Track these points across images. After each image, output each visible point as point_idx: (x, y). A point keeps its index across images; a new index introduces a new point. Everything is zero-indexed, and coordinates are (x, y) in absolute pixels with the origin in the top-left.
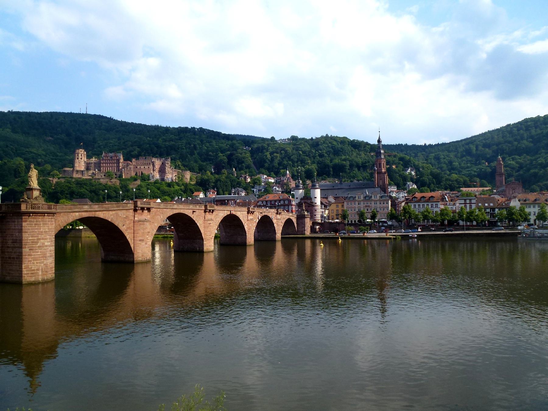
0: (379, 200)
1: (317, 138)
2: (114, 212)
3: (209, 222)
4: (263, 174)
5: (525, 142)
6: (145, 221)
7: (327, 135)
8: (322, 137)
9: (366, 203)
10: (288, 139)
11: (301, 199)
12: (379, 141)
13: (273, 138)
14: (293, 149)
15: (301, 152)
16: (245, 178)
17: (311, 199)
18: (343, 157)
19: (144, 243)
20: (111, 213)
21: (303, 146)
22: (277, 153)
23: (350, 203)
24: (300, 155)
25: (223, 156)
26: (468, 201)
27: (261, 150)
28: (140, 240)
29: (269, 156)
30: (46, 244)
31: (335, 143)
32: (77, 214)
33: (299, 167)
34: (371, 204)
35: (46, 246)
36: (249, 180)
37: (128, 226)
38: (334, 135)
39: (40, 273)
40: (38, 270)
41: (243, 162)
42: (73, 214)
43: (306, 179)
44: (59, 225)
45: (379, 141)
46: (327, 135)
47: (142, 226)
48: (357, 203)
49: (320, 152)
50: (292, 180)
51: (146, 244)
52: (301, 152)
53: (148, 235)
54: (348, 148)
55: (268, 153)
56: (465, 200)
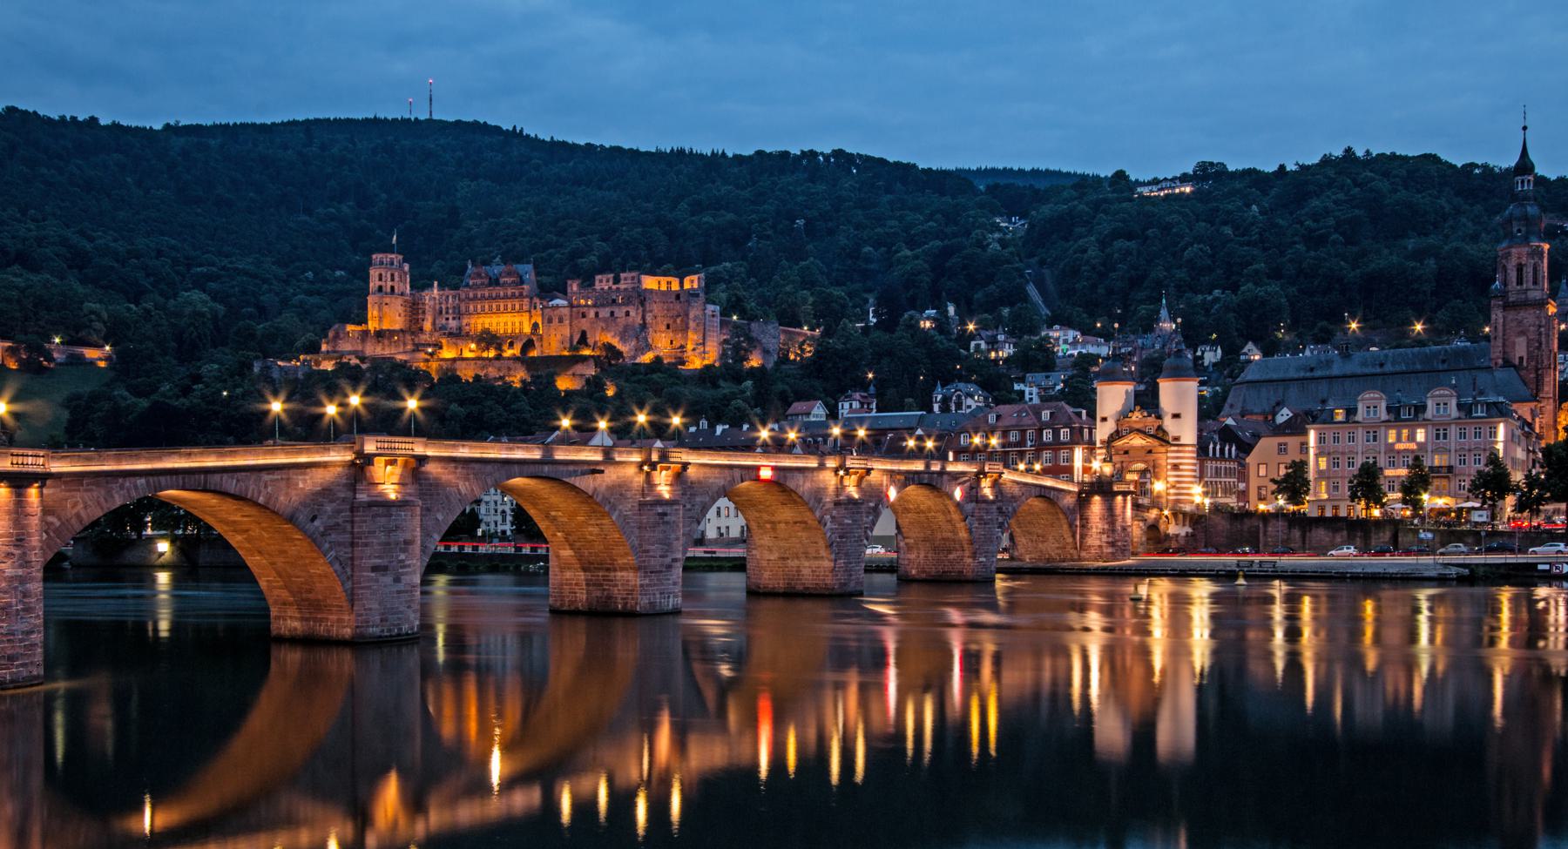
4: (1067, 323)
7: (1348, 150)
15: (1228, 230)
19: (388, 579)
25: (916, 257)
27: (1063, 227)
28: (375, 569)
29: (1093, 252)
33: (1217, 292)
46: (1348, 150)
51: (397, 580)
53: (404, 551)
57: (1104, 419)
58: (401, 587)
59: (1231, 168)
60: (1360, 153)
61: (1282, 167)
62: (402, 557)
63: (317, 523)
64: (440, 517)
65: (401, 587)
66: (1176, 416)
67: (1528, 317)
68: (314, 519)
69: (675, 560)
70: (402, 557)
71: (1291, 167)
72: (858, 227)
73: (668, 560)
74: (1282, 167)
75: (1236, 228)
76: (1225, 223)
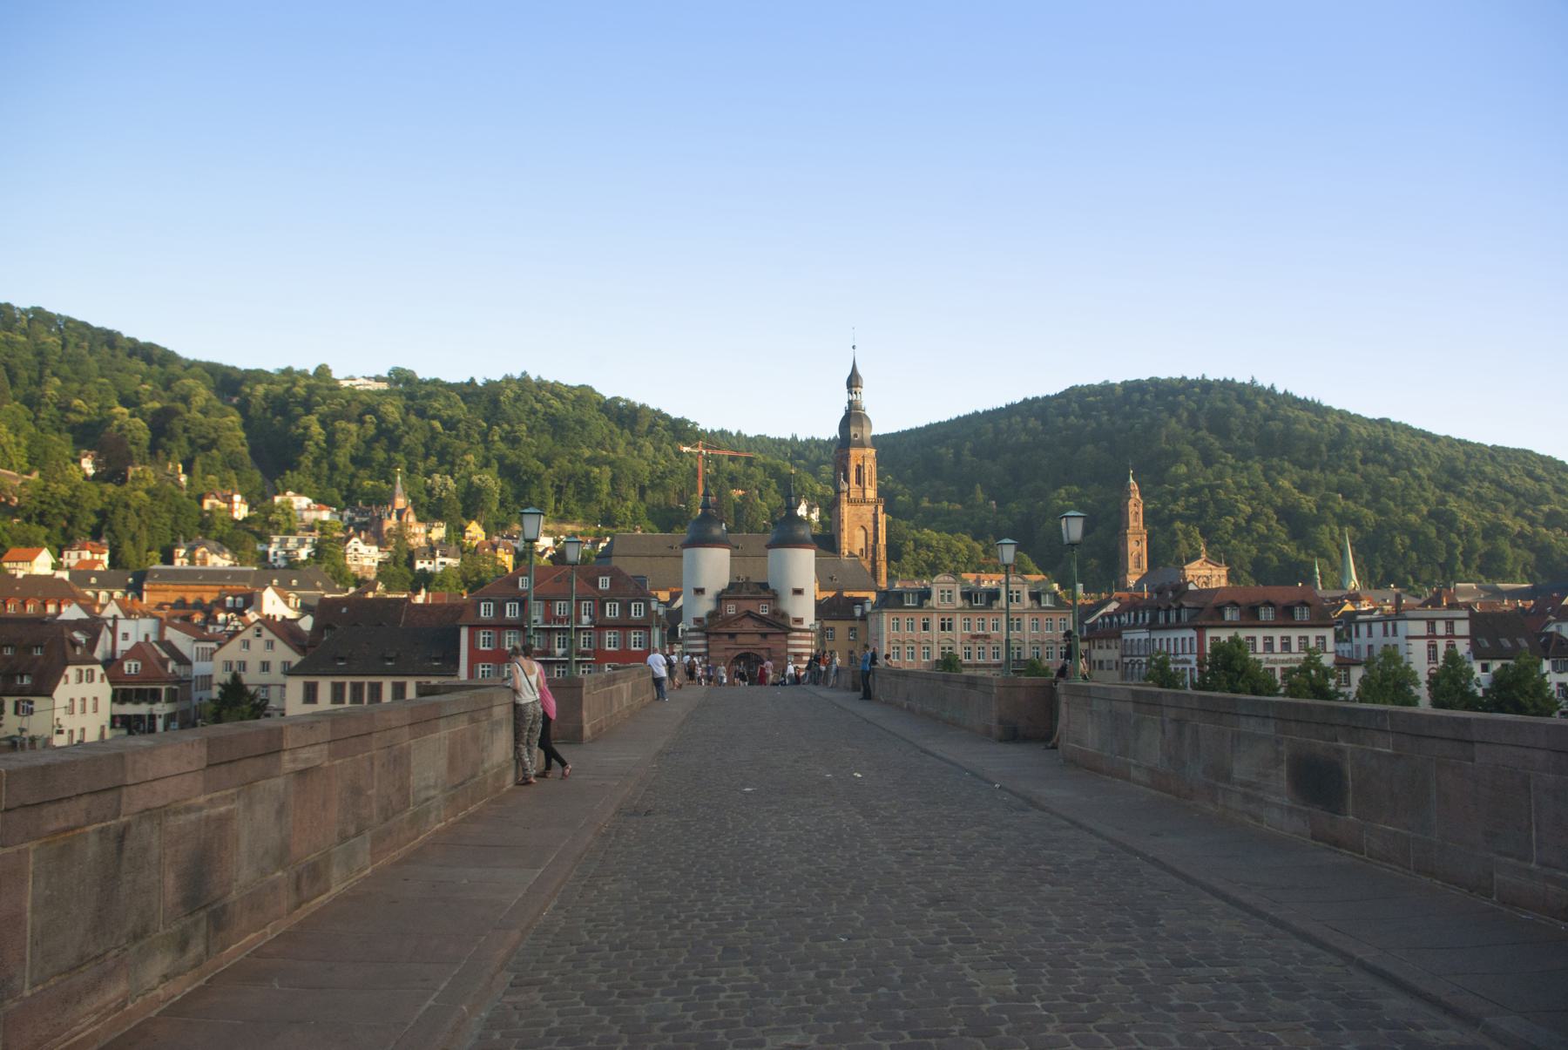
0: (1029, 611)
1: (489, 384)
5: (1090, 447)
7: (524, 373)
8: (508, 380)
9: (975, 620)
10: (378, 379)
11: (721, 598)
12: (853, 382)
13: (323, 371)
14: (407, 409)
15: (437, 424)
16: (230, 502)
17: (775, 597)
18: (587, 453)
21: (442, 401)
22: (349, 421)
23: (904, 619)
24: (434, 435)
25: (132, 416)
26: (1441, 628)
29: (316, 429)
31: (556, 403)
34: (996, 627)
36: (241, 511)
38: (550, 377)
41: (213, 444)
43: (465, 522)
45: (853, 382)
46: (524, 373)
48: (935, 622)
49: (506, 426)
50: (412, 519)
52: (437, 424)
54: (601, 426)
55: (314, 418)
56: (1431, 623)
57: (700, 591)
59: (420, 376)
60: (533, 377)
61: (472, 380)
66: (798, 592)
67: (867, 510)
71: (480, 382)
72: (65, 379)
74: (472, 380)
75: (443, 423)
76: (434, 417)
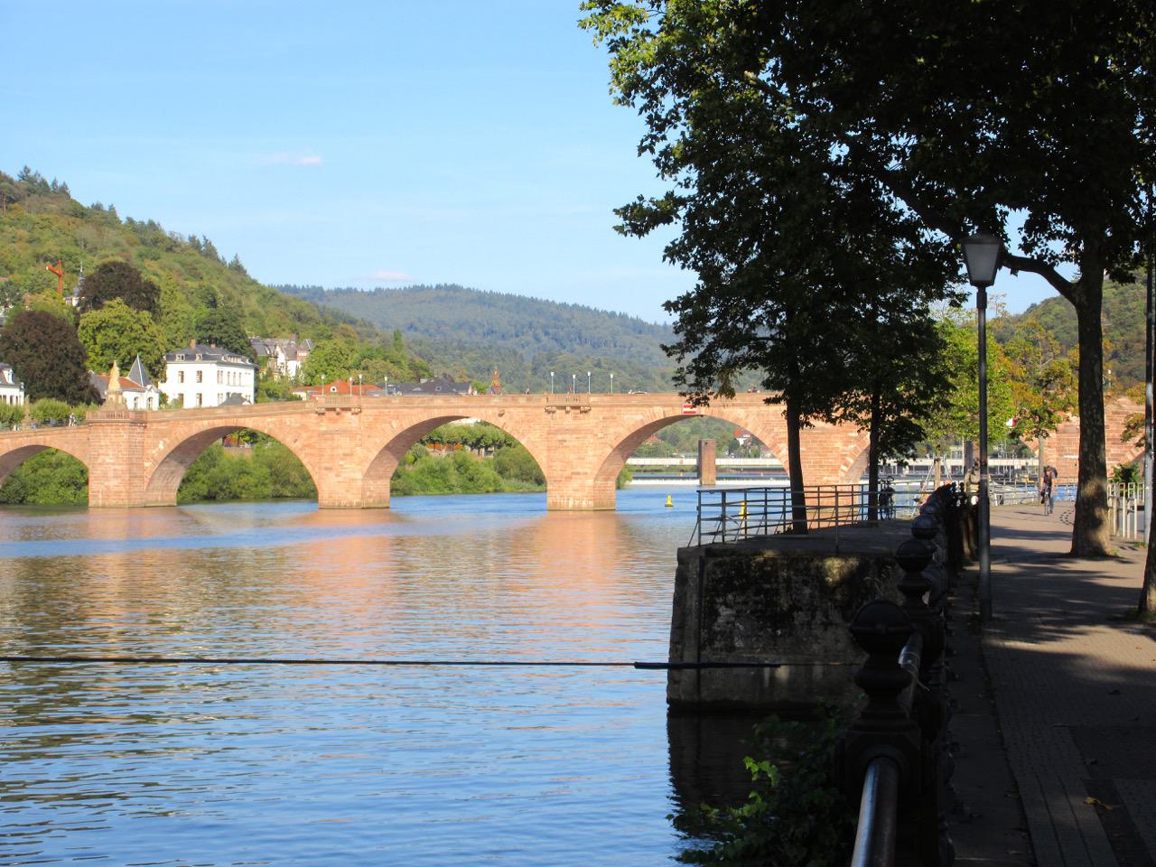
2: (273, 419)
3: (560, 437)
6: (344, 432)
19: (331, 475)
20: (269, 420)
28: (327, 469)
30: (108, 461)
32: (206, 422)
35: (108, 464)
37: (306, 443)
39: (100, 497)
40: (98, 492)
42: (200, 423)
44: (177, 438)
47: (329, 442)
53: (343, 459)
58: (340, 479)
62: (341, 463)
63: (298, 443)
64: (378, 441)
65: (340, 479)
68: (296, 441)
69: (578, 474)
70: (341, 463)
73: (568, 473)
